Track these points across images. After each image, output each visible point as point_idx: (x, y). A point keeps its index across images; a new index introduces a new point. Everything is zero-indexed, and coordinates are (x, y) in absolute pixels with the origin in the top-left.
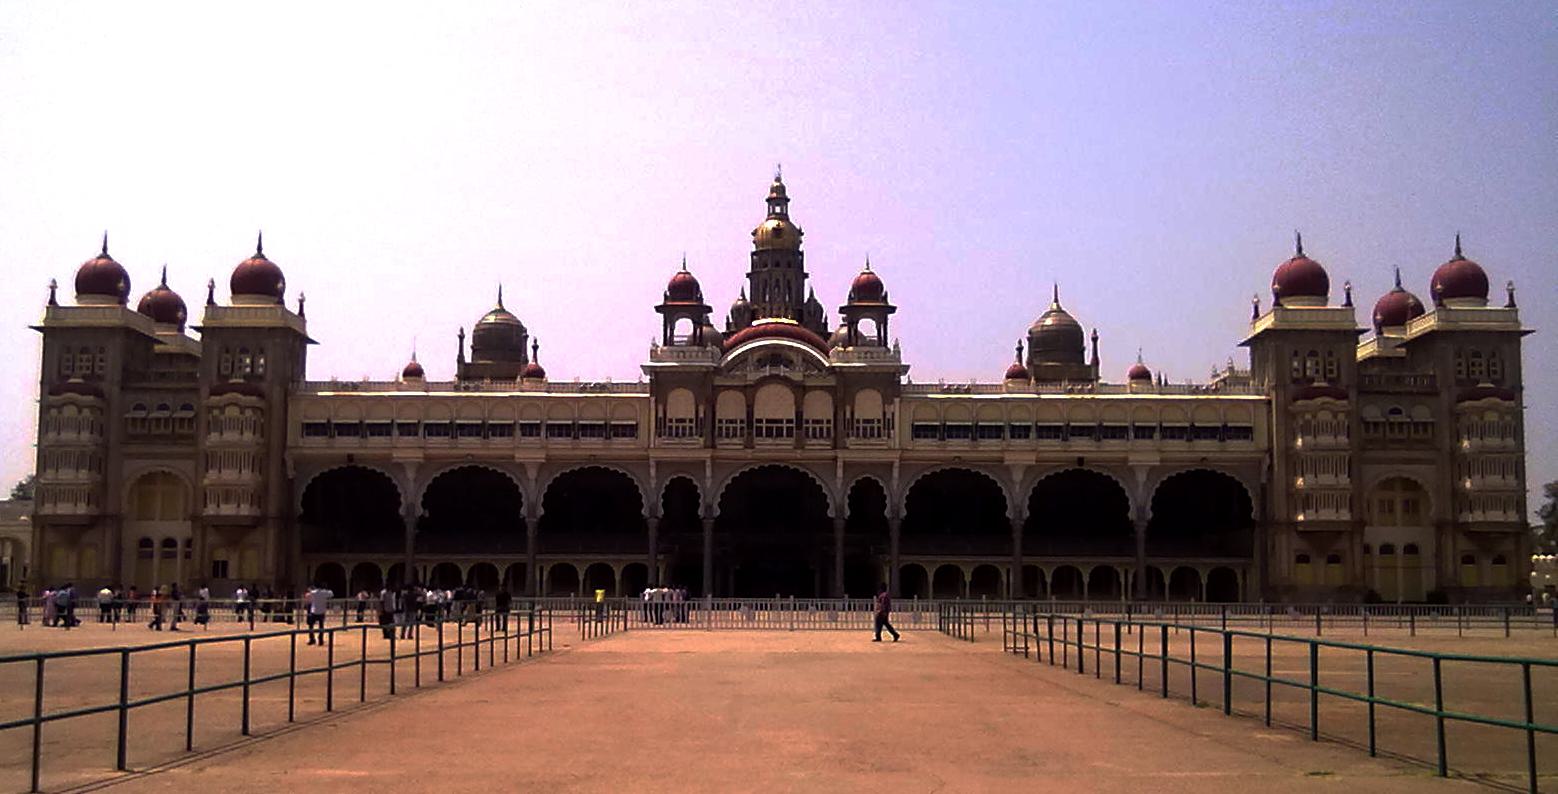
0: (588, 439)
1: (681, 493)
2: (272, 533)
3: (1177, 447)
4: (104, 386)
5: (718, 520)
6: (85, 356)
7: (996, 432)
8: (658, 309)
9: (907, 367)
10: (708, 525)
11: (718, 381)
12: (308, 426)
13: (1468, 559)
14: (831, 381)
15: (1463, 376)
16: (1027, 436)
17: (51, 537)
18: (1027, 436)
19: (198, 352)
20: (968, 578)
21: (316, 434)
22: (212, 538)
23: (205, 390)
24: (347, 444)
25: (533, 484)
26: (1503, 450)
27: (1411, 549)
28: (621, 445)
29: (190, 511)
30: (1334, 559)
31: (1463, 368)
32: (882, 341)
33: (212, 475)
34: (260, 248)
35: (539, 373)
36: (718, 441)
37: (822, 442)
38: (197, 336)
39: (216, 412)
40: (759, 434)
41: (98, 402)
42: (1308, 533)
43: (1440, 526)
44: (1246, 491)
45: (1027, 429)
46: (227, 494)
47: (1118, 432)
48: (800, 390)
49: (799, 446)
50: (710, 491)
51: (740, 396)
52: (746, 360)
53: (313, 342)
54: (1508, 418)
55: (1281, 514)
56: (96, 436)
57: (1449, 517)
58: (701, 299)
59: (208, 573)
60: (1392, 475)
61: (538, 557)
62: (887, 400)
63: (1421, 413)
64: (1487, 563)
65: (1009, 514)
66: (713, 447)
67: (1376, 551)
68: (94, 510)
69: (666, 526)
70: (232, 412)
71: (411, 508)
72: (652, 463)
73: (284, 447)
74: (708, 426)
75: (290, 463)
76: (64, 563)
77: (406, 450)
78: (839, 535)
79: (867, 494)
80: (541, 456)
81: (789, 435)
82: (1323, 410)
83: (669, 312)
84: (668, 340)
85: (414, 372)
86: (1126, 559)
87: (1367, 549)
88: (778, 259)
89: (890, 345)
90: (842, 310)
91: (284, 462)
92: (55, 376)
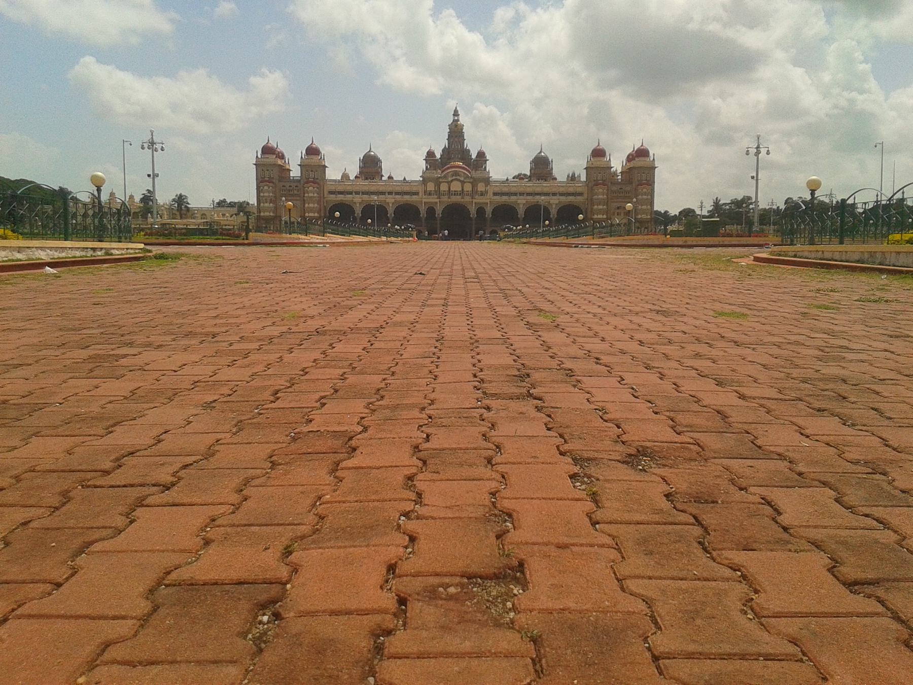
1: (431, 211)
3: (563, 198)
7: (515, 194)
24: (341, 197)
28: (415, 198)
46: (311, 210)
48: (463, 183)
50: (439, 210)
62: (486, 186)
63: (628, 188)
69: (426, 219)
70: (311, 188)
74: (438, 193)
77: (357, 199)
78: (474, 222)
79: (481, 211)
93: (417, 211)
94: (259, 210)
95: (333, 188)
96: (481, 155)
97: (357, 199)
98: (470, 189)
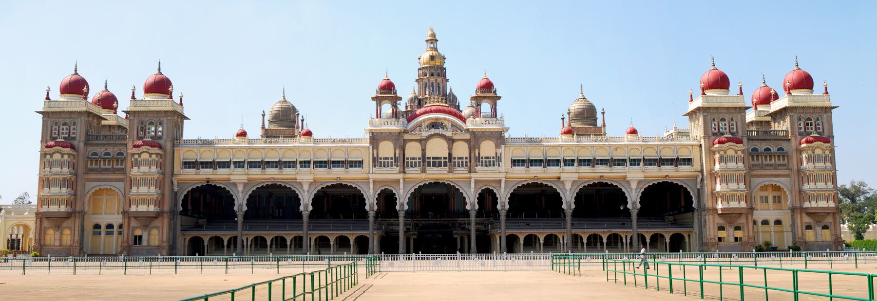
0: (337, 169)
1: (387, 198)
2: (166, 221)
4: (75, 143)
5: (407, 212)
6: (65, 127)
7: (557, 162)
8: (373, 99)
9: (507, 129)
10: (401, 215)
11: (406, 137)
12: (185, 163)
13: (809, 227)
14: (468, 136)
15: (803, 130)
16: (573, 165)
17: (46, 223)
18: (573, 165)
19: (126, 124)
20: (542, 241)
21: (190, 167)
22: (134, 223)
23: (130, 145)
24: (206, 174)
25: (306, 193)
26: (825, 169)
27: (778, 222)
29: (121, 210)
30: (738, 228)
31: (802, 126)
32: (494, 114)
33: (134, 189)
34: (159, 69)
35: (309, 134)
36: (406, 169)
37: (462, 169)
38: (124, 115)
39: (136, 156)
40: (429, 165)
41: (72, 152)
42: (725, 214)
43: (793, 210)
44: (689, 193)
45: (573, 161)
47: (621, 162)
48: (451, 141)
49: (451, 171)
51: (417, 145)
52: (420, 126)
53: (187, 119)
54: (827, 152)
55: (709, 204)
56: (71, 170)
57: (798, 205)
58: (395, 93)
59: (131, 242)
60: (766, 183)
61: (309, 232)
62: (498, 146)
64: (819, 229)
65: (564, 206)
66: (404, 172)
67: (760, 223)
68: (69, 209)
69: (378, 214)
70: (145, 156)
71: (241, 206)
72: (371, 181)
73: (173, 175)
74: (402, 162)
75: (175, 183)
76: (51, 237)
77: (238, 176)
79: (487, 197)
80: (310, 178)
81: (445, 165)
82: (731, 150)
83: (378, 100)
84: (379, 115)
85: (243, 134)
86: (625, 230)
87: (755, 223)
88: (434, 73)
89: (498, 117)
90: (473, 98)
91: (172, 182)
92: (49, 138)
93: (358, 198)
94: (42, 201)
95: (191, 157)
96: (488, 86)
97: (238, 176)
98: (466, 154)
